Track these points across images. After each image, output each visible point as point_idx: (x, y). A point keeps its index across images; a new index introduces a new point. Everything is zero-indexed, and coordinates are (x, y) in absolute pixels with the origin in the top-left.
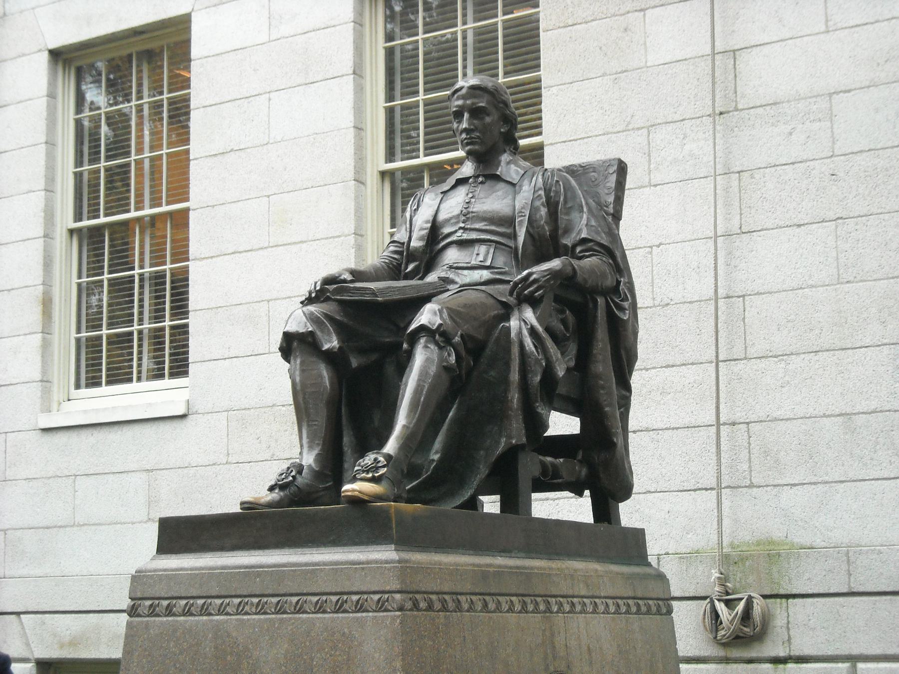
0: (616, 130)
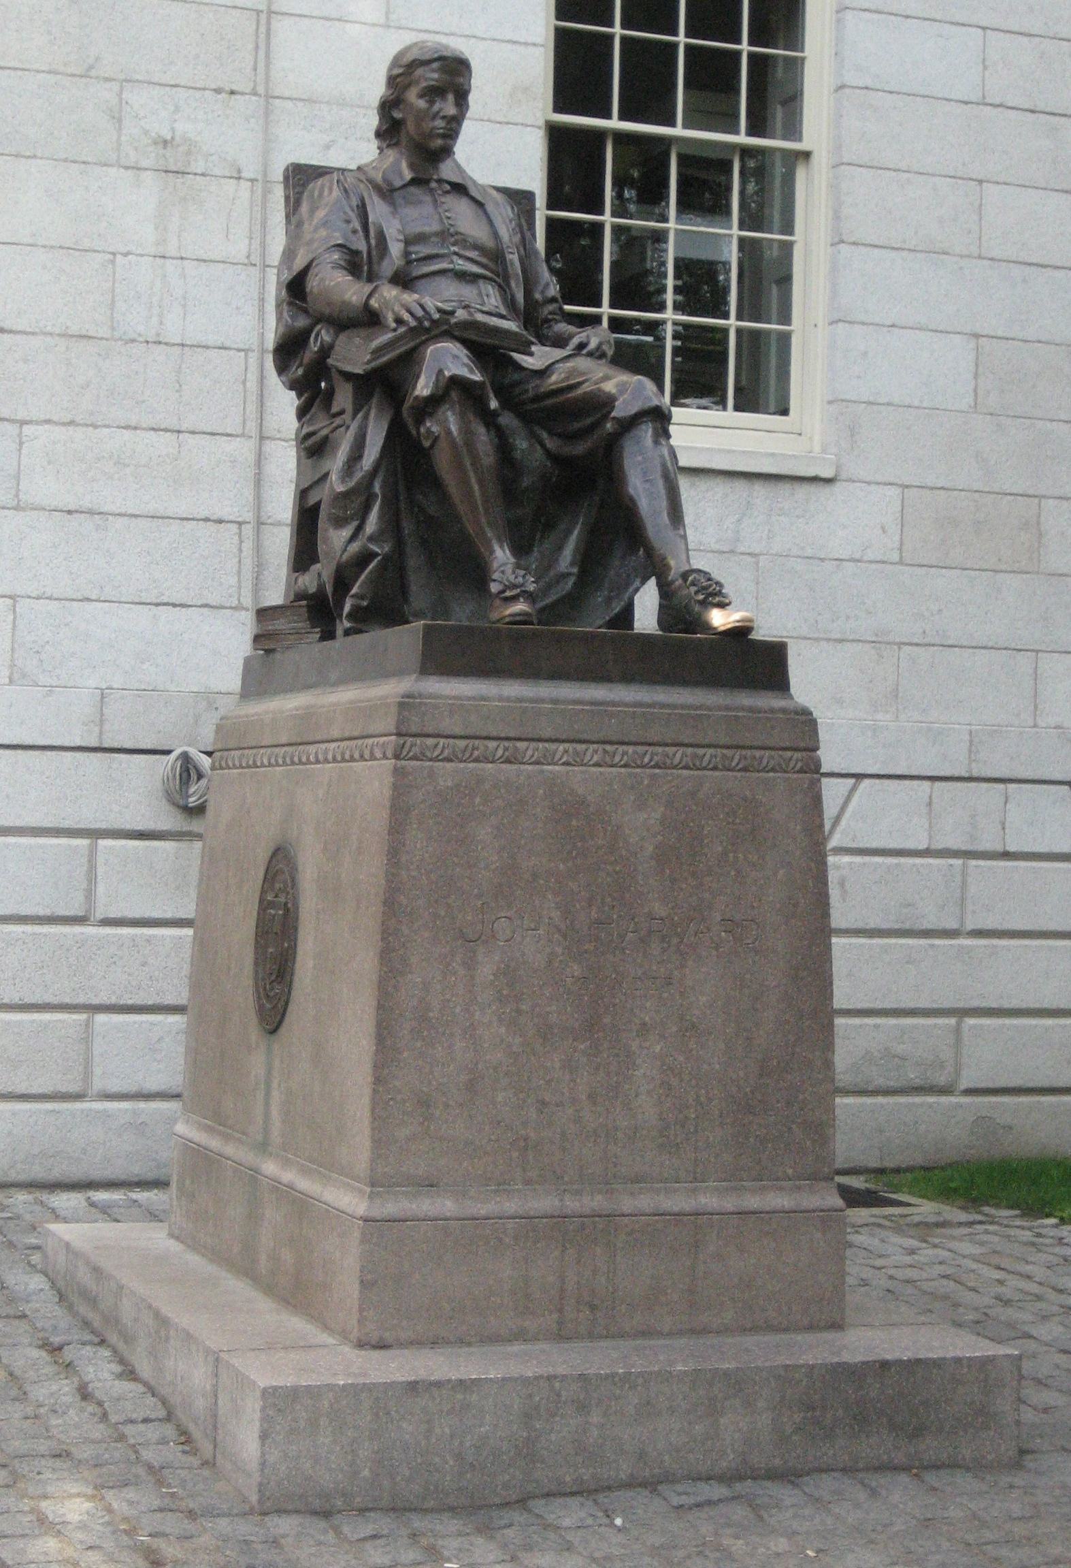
0: (69, 71)
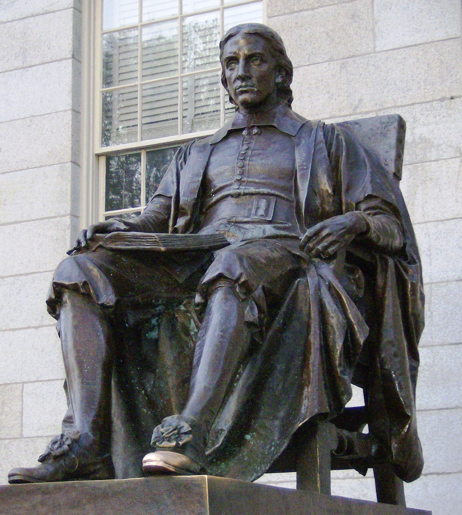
0: (343, 114)
